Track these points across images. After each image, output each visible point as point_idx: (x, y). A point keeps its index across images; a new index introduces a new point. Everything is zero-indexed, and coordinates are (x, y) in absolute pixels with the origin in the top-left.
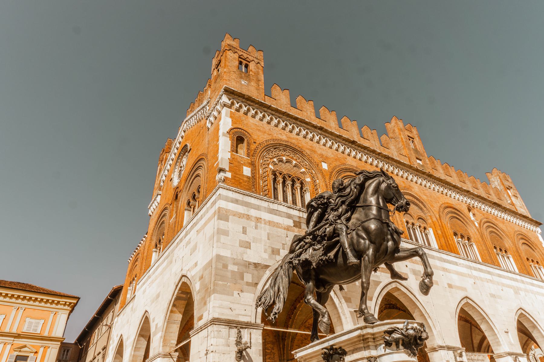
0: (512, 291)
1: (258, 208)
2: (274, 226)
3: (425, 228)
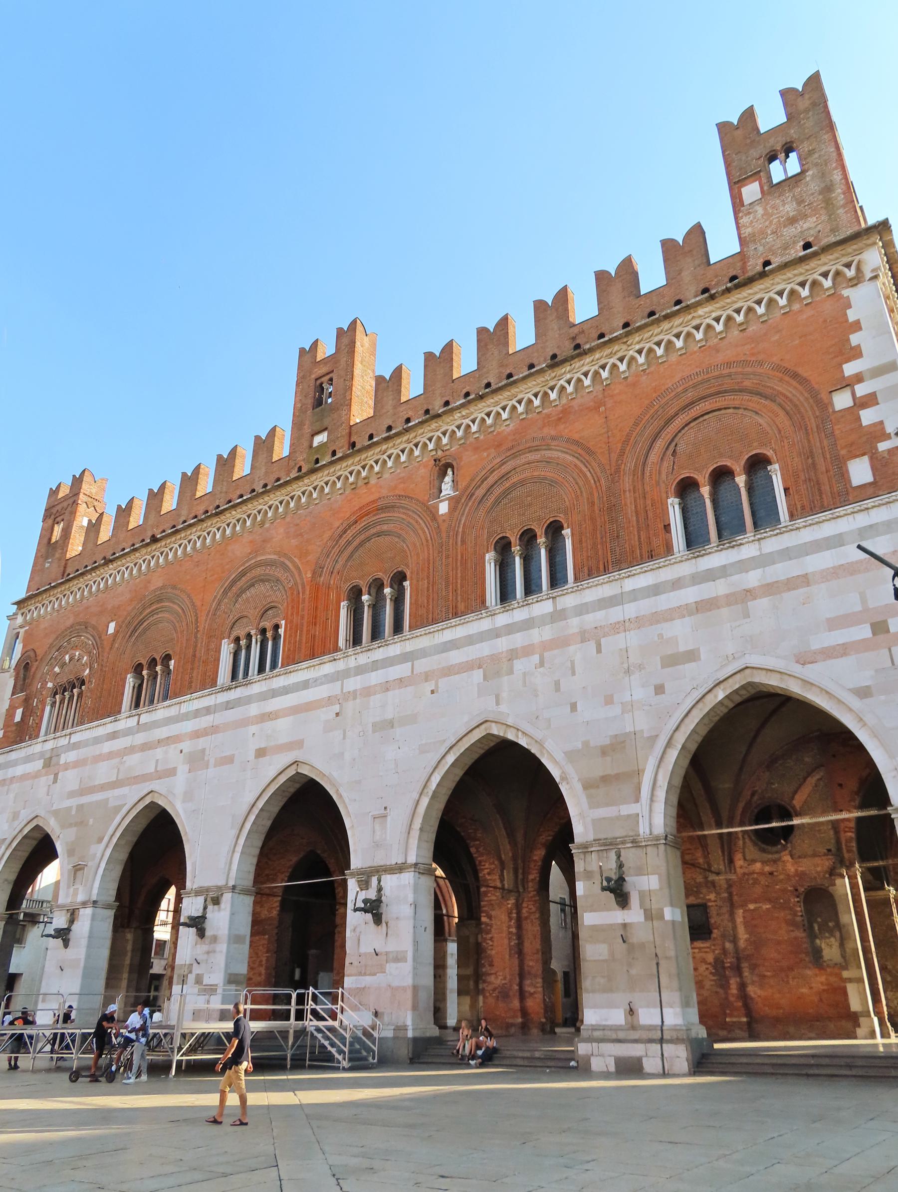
0: (477, 675)
1: (14, 764)
3: (277, 627)
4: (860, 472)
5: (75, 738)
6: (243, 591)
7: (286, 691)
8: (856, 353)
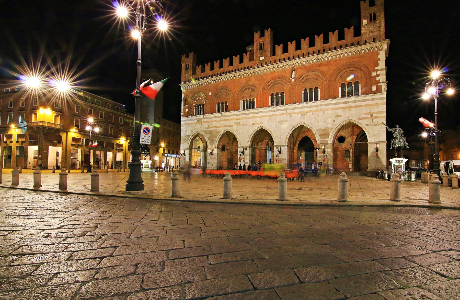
0: (300, 115)
1: (189, 120)
4: (374, 88)
6: (244, 90)
7: (258, 113)
8: (378, 65)
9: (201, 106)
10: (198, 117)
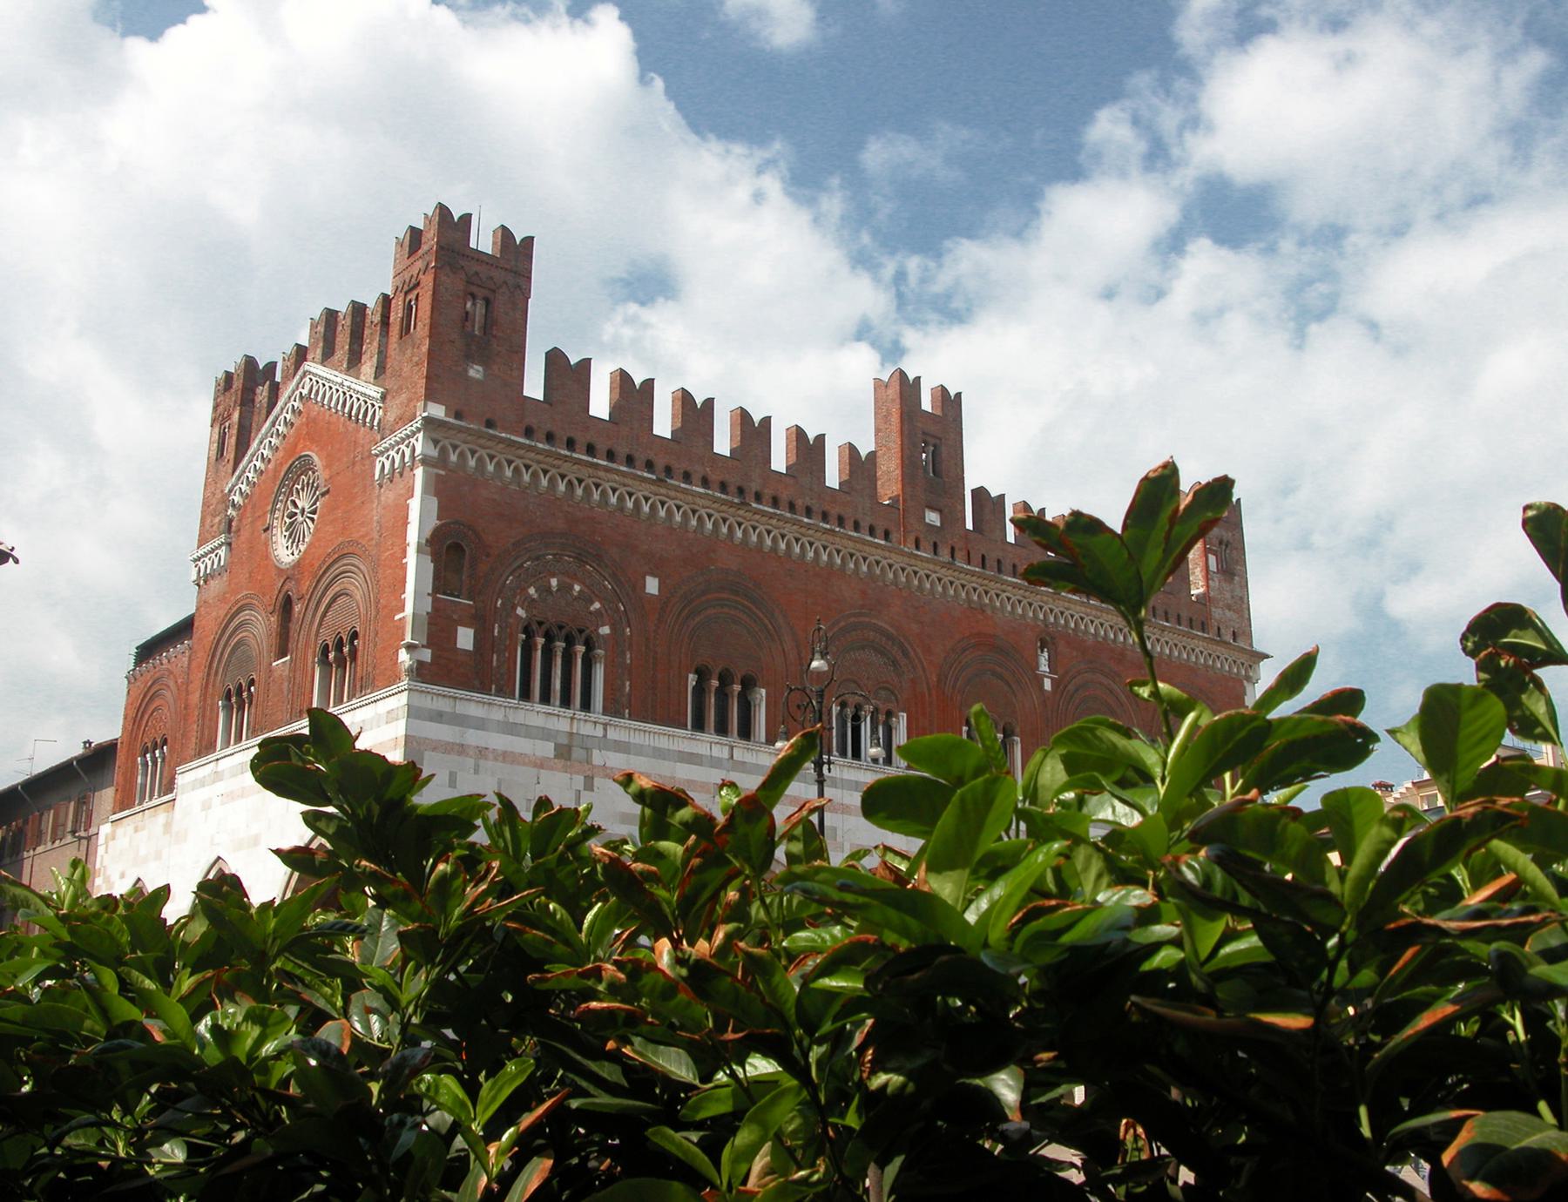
1: (481, 724)
2: (512, 762)
3: (889, 714)
5: (612, 734)
9: (570, 641)
10: (559, 721)
